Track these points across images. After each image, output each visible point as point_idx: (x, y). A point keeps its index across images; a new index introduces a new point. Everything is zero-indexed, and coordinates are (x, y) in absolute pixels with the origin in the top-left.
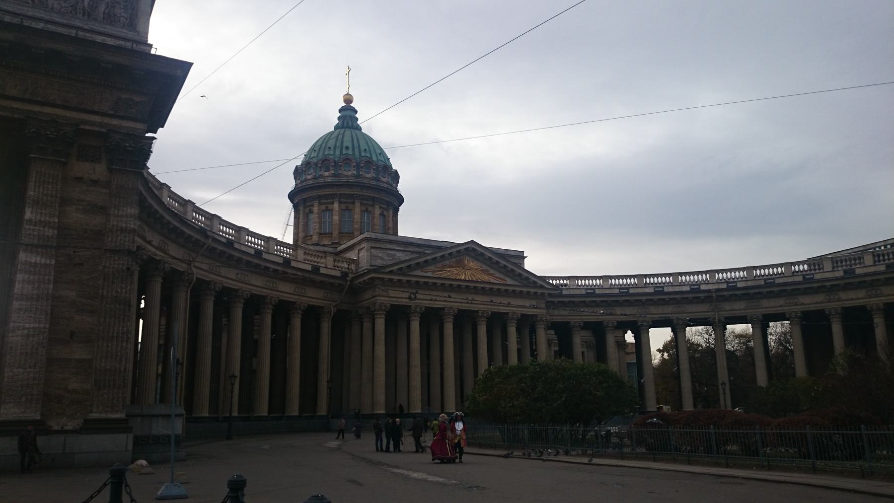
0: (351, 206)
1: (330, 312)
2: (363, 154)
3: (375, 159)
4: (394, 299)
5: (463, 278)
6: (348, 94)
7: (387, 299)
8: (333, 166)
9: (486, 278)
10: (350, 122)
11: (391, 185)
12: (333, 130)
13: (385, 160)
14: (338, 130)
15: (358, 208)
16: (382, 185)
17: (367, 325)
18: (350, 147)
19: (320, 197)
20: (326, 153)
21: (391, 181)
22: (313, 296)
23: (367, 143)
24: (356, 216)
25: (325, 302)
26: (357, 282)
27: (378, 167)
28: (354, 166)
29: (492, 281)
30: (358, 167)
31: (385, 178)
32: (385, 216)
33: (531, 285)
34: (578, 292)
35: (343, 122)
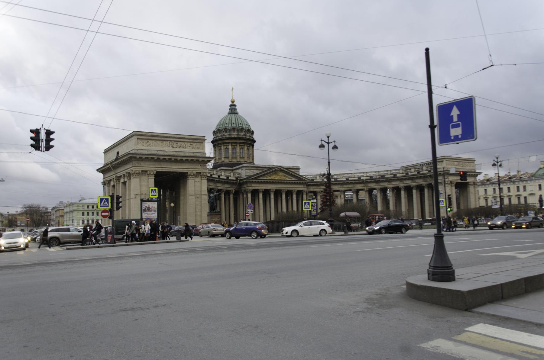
1: (233, 192)
2: (240, 126)
3: (244, 127)
5: (277, 179)
6: (233, 99)
8: (228, 131)
10: (234, 111)
11: (251, 137)
14: (230, 115)
16: (247, 137)
17: (245, 196)
18: (234, 122)
19: (224, 143)
20: (226, 125)
21: (251, 135)
22: (227, 187)
23: (241, 121)
26: (241, 181)
27: (246, 130)
28: (237, 131)
29: (288, 179)
30: (238, 131)
35: (231, 111)
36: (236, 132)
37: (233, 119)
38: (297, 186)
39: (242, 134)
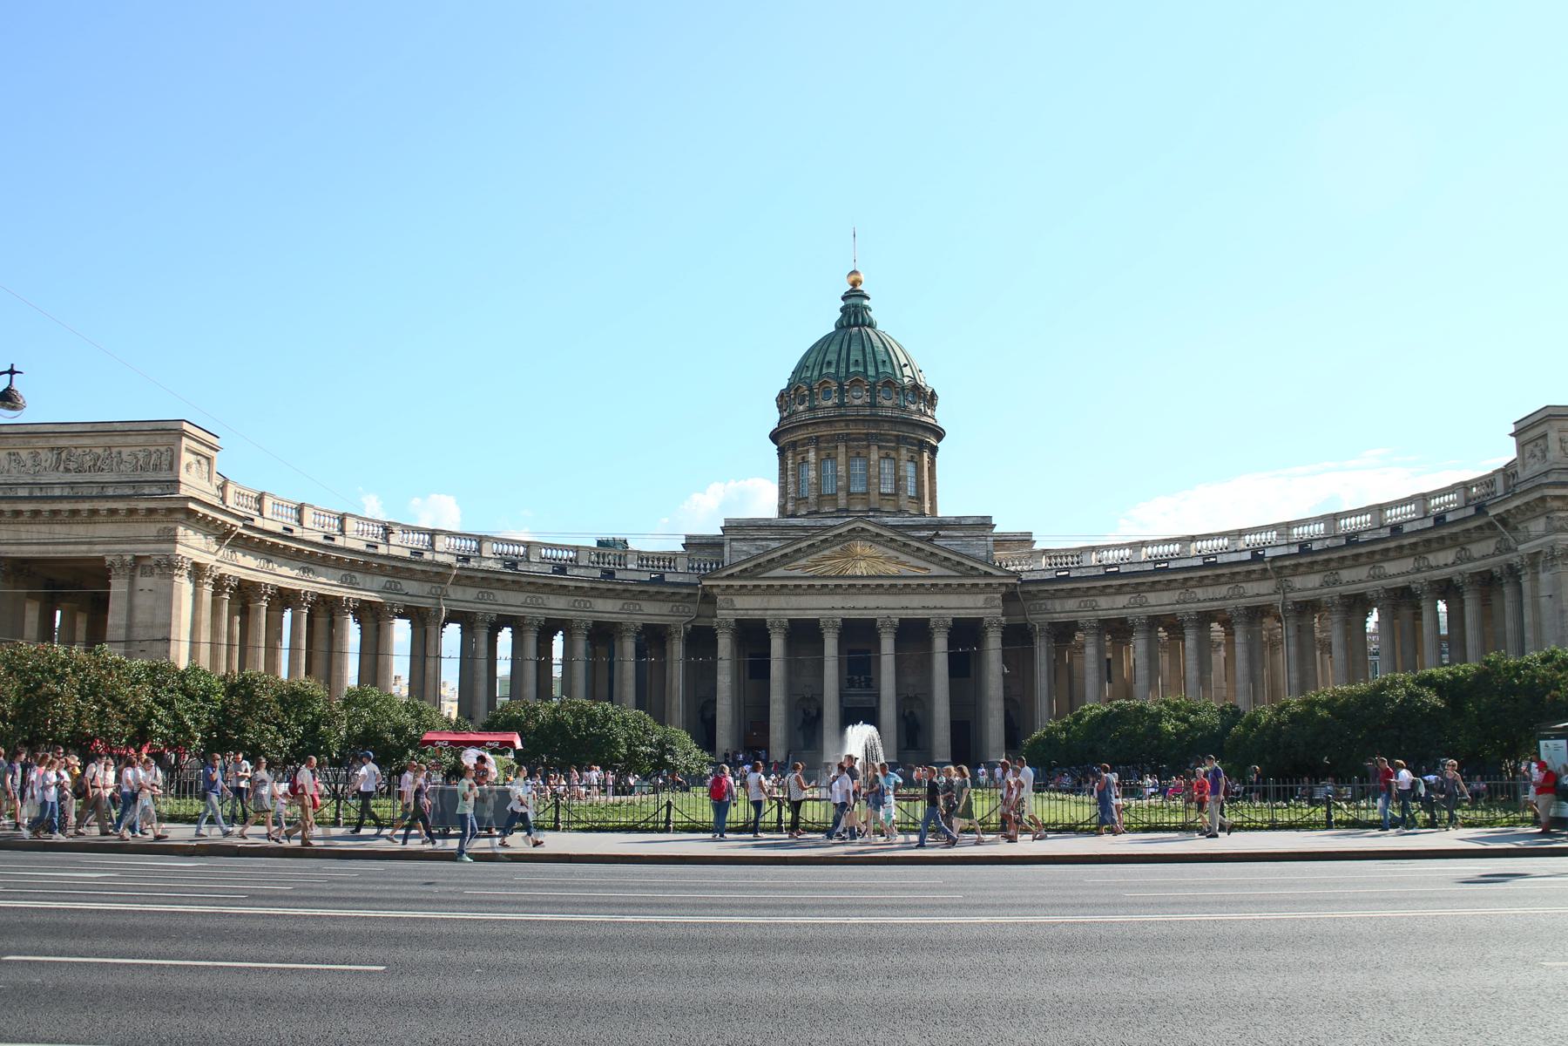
0: (833, 452)
3: (871, 371)
4: (742, 612)
7: (732, 612)
9: (893, 569)
12: (834, 330)
15: (841, 458)
19: (794, 445)
20: (803, 376)
24: (839, 467)
25: (675, 618)
28: (835, 391)
29: (905, 571)
32: (894, 459)
33: (974, 573)
34: (1094, 572)
36: (834, 395)
37: (834, 348)
38: (952, 600)
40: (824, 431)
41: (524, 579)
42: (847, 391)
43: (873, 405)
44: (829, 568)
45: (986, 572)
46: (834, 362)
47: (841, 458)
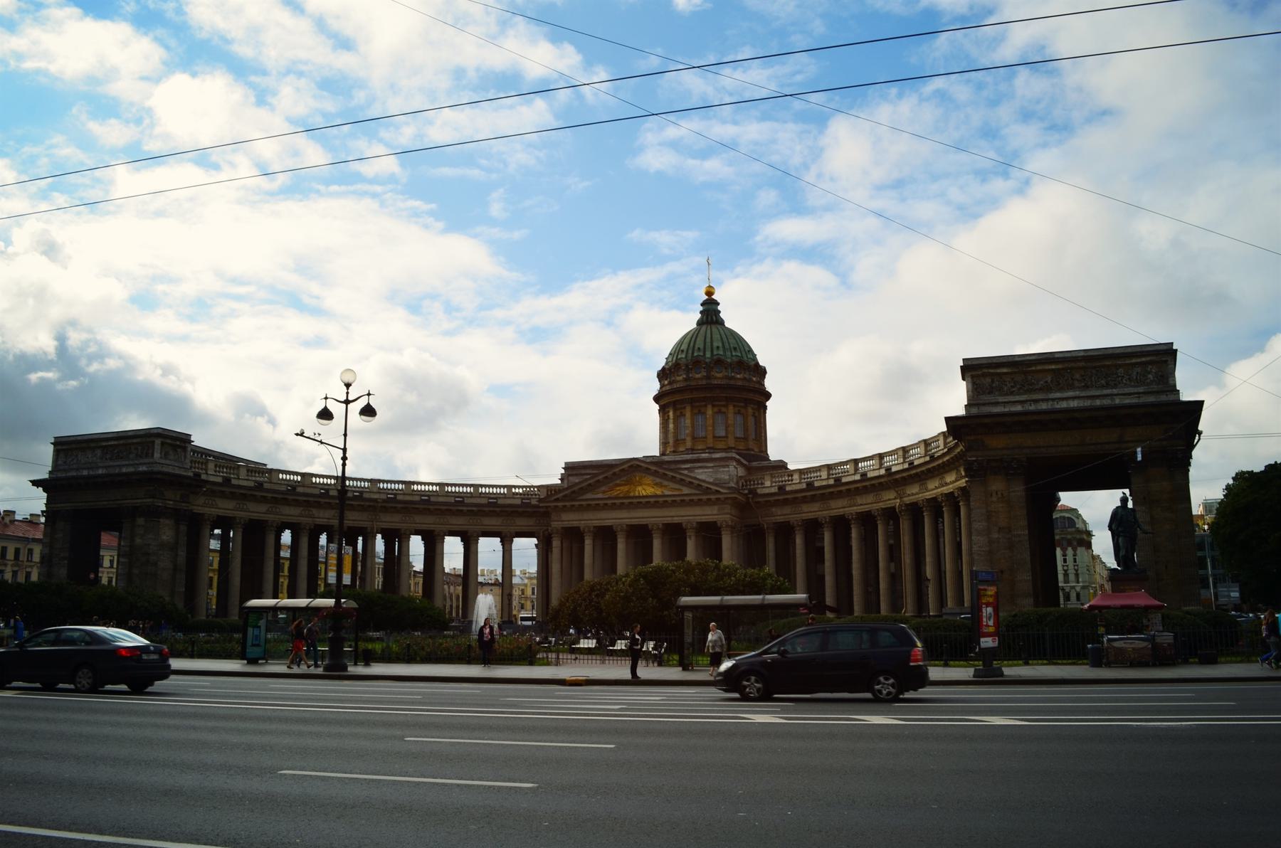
2: (695, 354)
3: (708, 355)
5: (632, 494)
6: (710, 287)
7: (560, 523)
9: (659, 493)
13: (724, 351)
15: (688, 414)
24: (686, 422)
28: (684, 370)
29: (667, 493)
30: (688, 370)
31: (721, 372)
32: (725, 413)
37: (687, 340)
39: (698, 376)
40: (677, 397)
41: (431, 507)
42: (691, 369)
43: (708, 377)
44: (619, 492)
45: (717, 491)
46: (685, 350)
47: (688, 414)
